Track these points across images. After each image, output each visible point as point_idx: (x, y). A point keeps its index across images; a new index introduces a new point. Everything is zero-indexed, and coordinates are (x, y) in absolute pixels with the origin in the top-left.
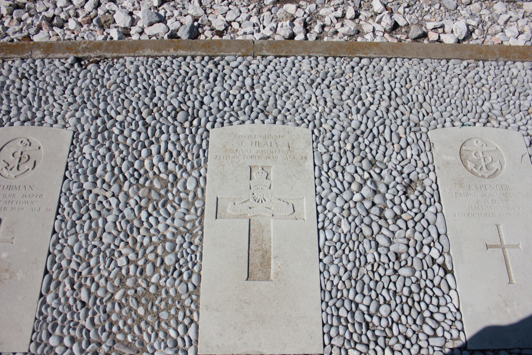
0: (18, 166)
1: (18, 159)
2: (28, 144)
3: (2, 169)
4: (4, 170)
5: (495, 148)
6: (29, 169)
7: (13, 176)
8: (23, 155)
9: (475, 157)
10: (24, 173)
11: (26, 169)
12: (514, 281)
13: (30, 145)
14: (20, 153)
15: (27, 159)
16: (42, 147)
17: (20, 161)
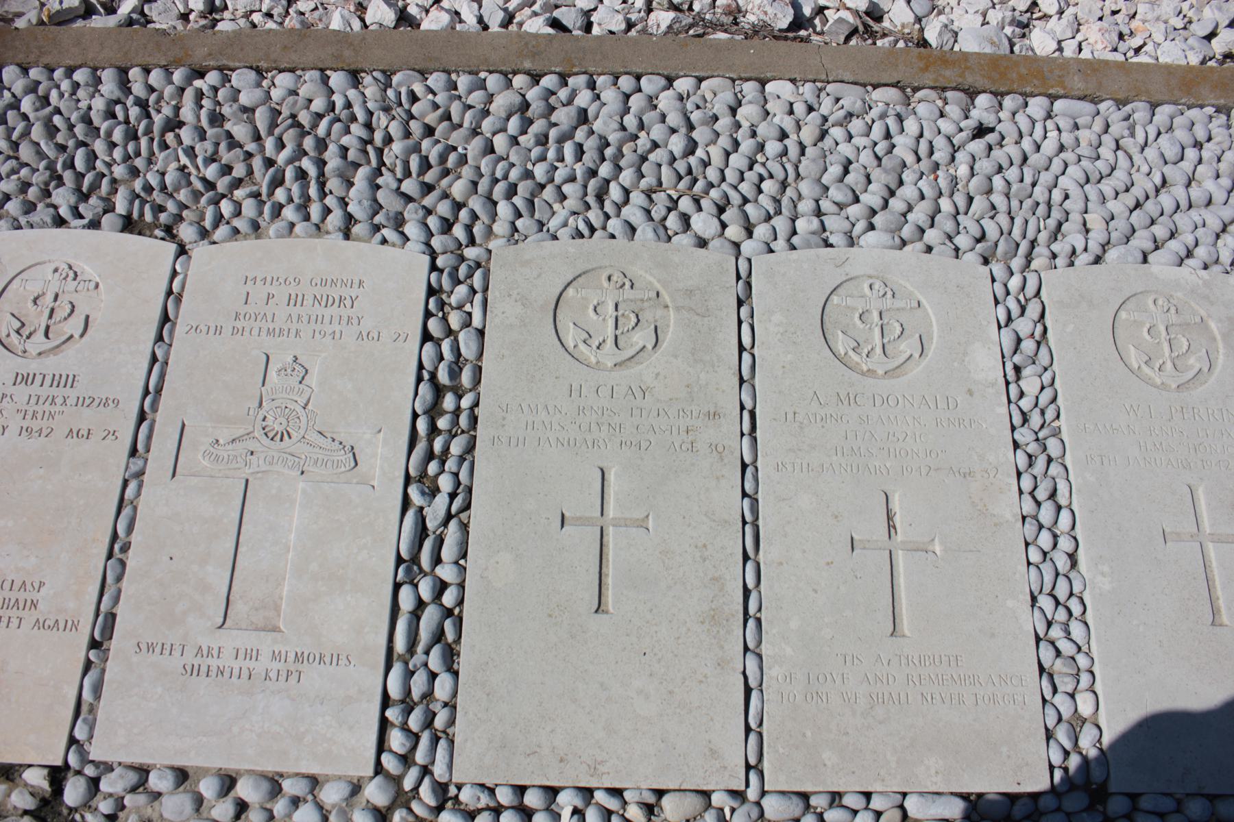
0: (616, 337)
1: (611, 323)
2: (628, 284)
3: (8, 335)
4: (582, 347)
5: (1198, 320)
6: (644, 347)
7: (610, 364)
8: (620, 313)
9: (1148, 337)
10: (58, 347)
11: (638, 348)
12: (1225, 619)
13: (632, 287)
14: (611, 307)
15: (68, 311)
16: (663, 292)
17: (616, 328)
